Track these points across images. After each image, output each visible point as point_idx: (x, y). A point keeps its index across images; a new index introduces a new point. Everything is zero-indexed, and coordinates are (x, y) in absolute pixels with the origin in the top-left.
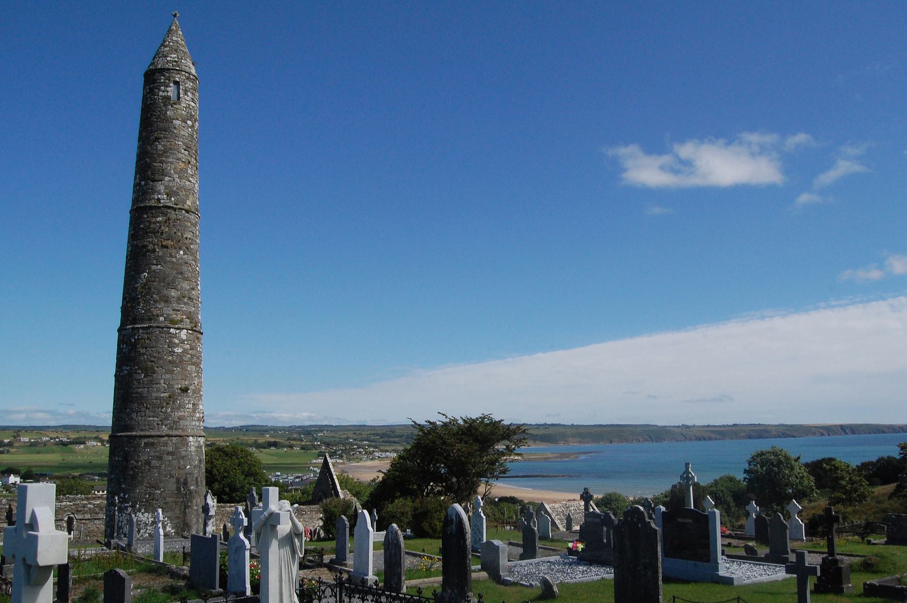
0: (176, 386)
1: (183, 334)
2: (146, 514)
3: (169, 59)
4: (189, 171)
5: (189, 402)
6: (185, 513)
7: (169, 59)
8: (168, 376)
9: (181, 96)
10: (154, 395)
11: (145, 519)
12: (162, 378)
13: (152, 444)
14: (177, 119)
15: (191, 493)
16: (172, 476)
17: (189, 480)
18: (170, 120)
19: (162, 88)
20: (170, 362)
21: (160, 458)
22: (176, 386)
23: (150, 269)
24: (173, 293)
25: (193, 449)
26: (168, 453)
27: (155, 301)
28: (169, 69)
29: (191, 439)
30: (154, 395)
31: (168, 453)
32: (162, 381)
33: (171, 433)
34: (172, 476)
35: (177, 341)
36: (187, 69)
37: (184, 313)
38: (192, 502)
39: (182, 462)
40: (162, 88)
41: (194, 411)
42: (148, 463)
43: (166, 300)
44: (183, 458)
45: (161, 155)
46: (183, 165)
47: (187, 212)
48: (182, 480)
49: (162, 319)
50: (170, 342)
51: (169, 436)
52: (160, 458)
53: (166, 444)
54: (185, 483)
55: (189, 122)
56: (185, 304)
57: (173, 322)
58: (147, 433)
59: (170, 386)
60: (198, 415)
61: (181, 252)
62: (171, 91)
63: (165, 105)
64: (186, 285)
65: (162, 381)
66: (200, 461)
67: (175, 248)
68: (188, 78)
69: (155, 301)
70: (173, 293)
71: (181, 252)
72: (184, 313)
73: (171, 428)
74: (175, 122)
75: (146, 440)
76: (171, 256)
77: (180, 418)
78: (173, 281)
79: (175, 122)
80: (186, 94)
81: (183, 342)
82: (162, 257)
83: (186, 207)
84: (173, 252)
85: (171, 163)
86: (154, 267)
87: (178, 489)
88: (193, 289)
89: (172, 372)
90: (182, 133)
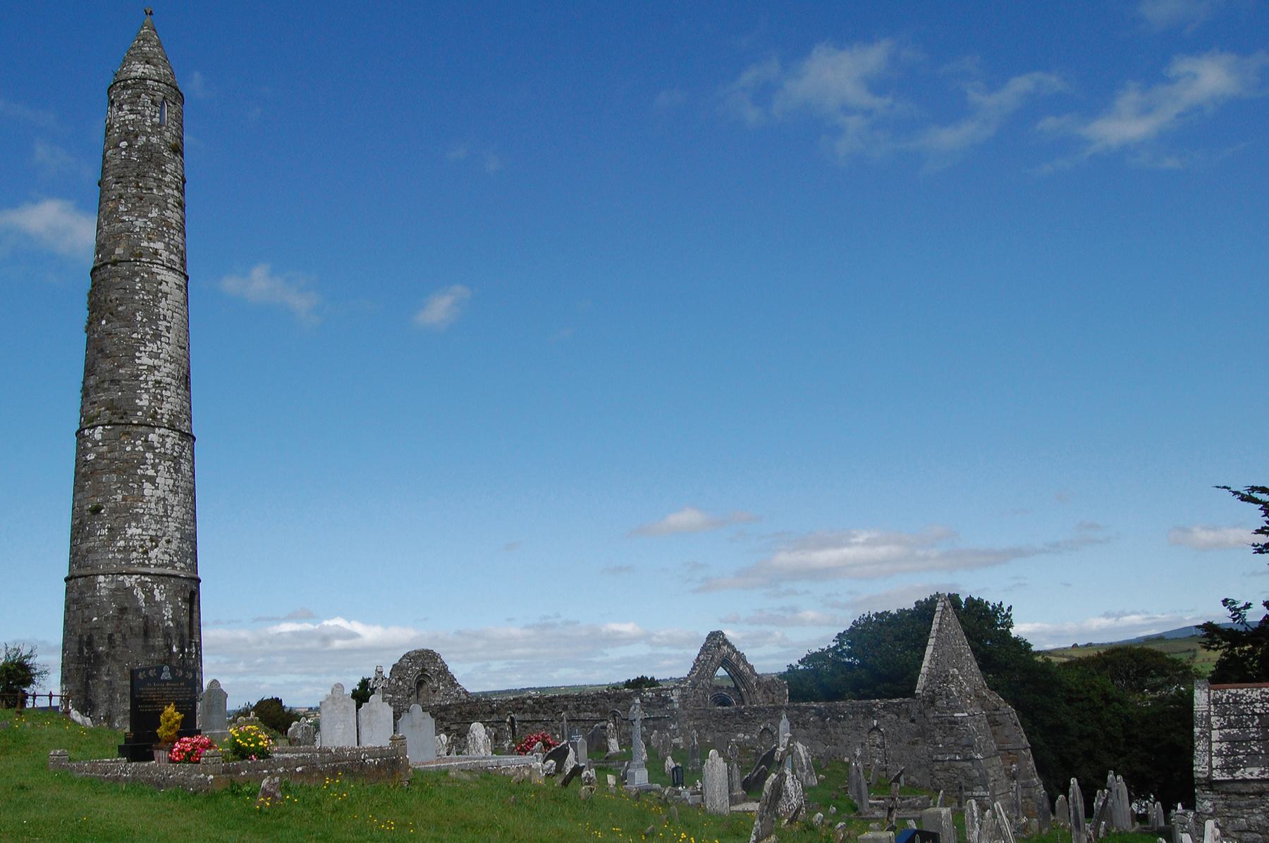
4: (122, 208)
5: (103, 527)
6: (87, 684)
17: (96, 638)
29: (101, 578)
38: (98, 670)
39: (86, 612)
48: (85, 638)
54: (90, 643)
55: (124, 144)
56: (105, 390)
61: (104, 322)
71: (104, 322)
72: (103, 403)
77: (89, 551)
81: (96, 444)
83: (113, 257)
87: (81, 651)
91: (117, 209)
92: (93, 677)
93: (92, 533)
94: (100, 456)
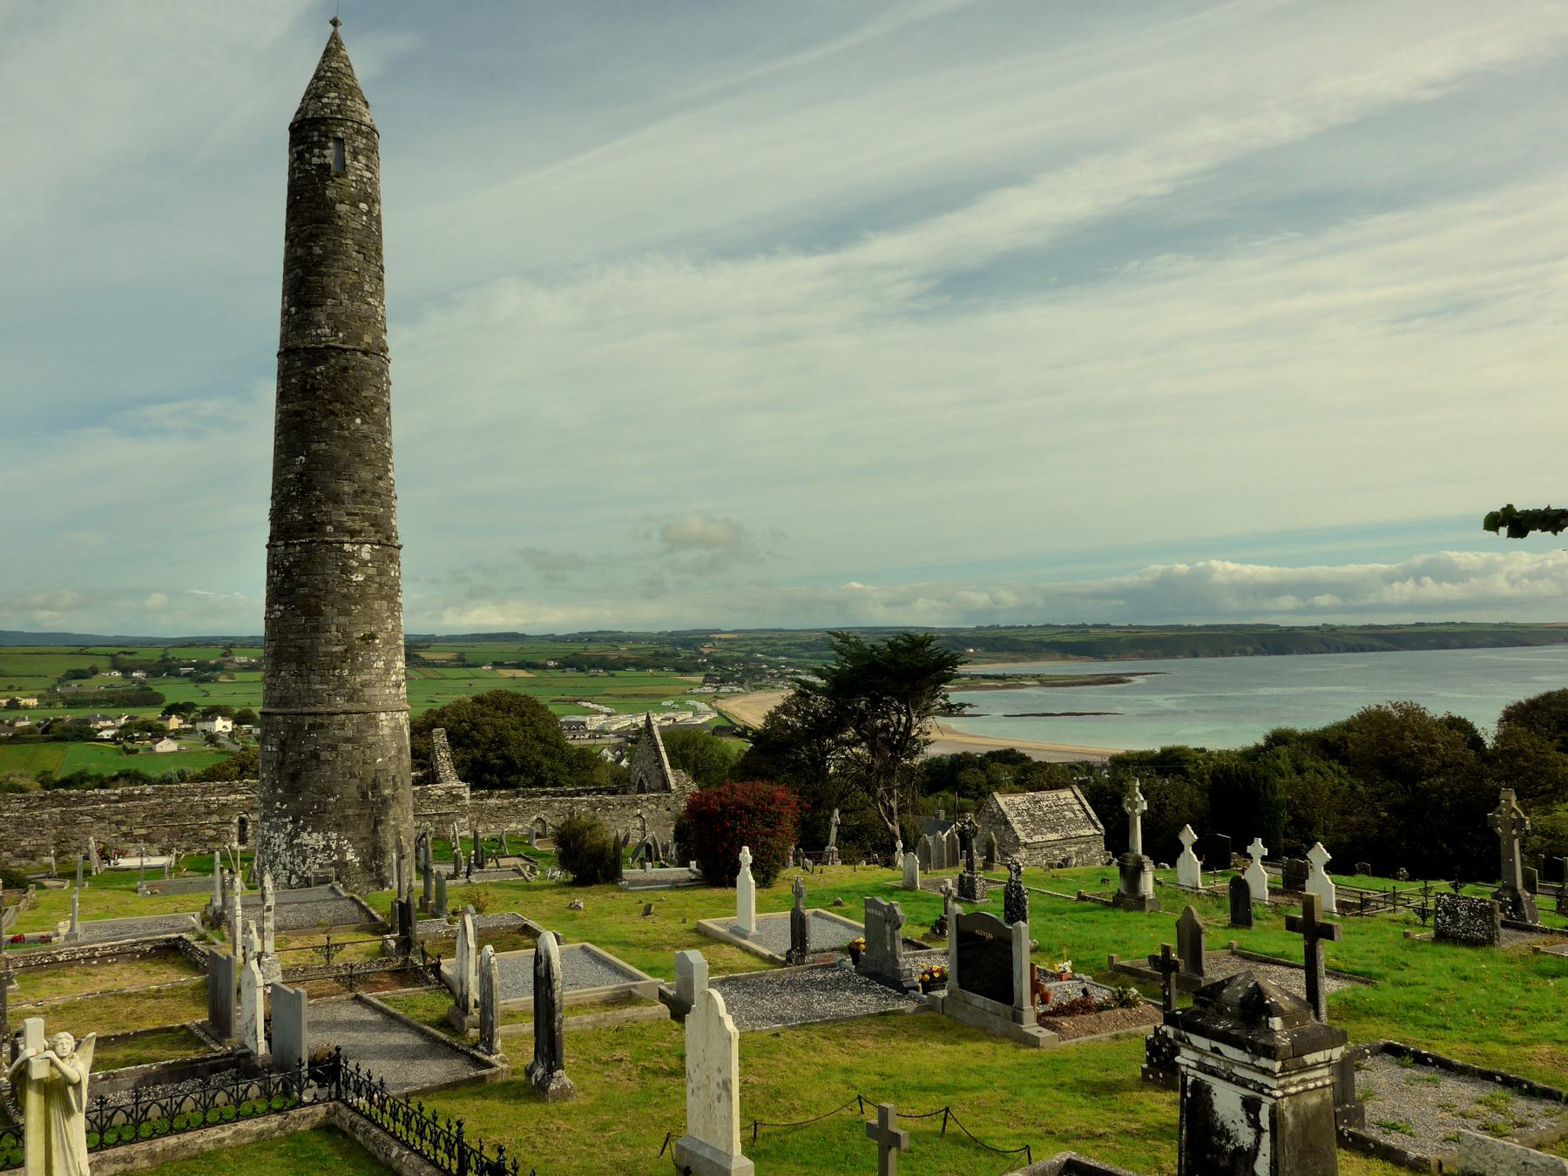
0: (356, 635)
1: (366, 552)
2: (315, 835)
3: (325, 100)
4: (366, 287)
5: (379, 657)
6: (375, 831)
7: (325, 100)
8: (342, 620)
9: (348, 162)
10: (322, 649)
11: (312, 842)
12: (334, 621)
13: (322, 726)
14: (342, 202)
15: (385, 801)
16: (353, 776)
18: (330, 205)
19: (316, 151)
20: (344, 596)
21: (334, 748)
22: (356, 635)
23: (309, 449)
24: (347, 488)
25: (386, 731)
26: (347, 740)
27: (319, 501)
28: (324, 119)
29: (383, 716)
30: (322, 649)
31: (347, 740)
32: (334, 628)
33: (348, 706)
34: (353, 776)
35: (355, 564)
36: (356, 117)
37: (365, 517)
38: (386, 814)
40: (316, 151)
41: (387, 671)
42: (315, 755)
43: (337, 499)
44: (370, 746)
45: (320, 264)
46: (355, 277)
47: (365, 353)
48: (369, 781)
49: (329, 528)
50: (345, 564)
51: (345, 713)
52: (334, 748)
53: (342, 726)
54: (375, 786)
55: (363, 206)
57: (353, 533)
58: (314, 710)
59: (346, 635)
60: (394, 678)
62: (330, 154)
63: (323, 180)
64: (366, 474)
65: (334, 628)
66: (400, 750)
67: (347, 415)
68: (359, 132)
69: (319, 501)
70: (347, 488)
71: (358, 421)
72: (365, 517)
73: (350, 699)
74: (339, 207)
75: (309, 720)
76: (341, 427)
78: (346, 467)
79: (339, 207)
80: (355, 158)
81: (364, 563)
82: (328, 431)
83: (363, 346)
84: (343, 420)
85: (335, 275)
86: (314, 446)
87: (364, 795)
88: (380, 478)
89: (348, 613)
90: (353, 224)
91: (361, 284)
92: (381, 822)
93: (367, 665)
94: (369, 578)
